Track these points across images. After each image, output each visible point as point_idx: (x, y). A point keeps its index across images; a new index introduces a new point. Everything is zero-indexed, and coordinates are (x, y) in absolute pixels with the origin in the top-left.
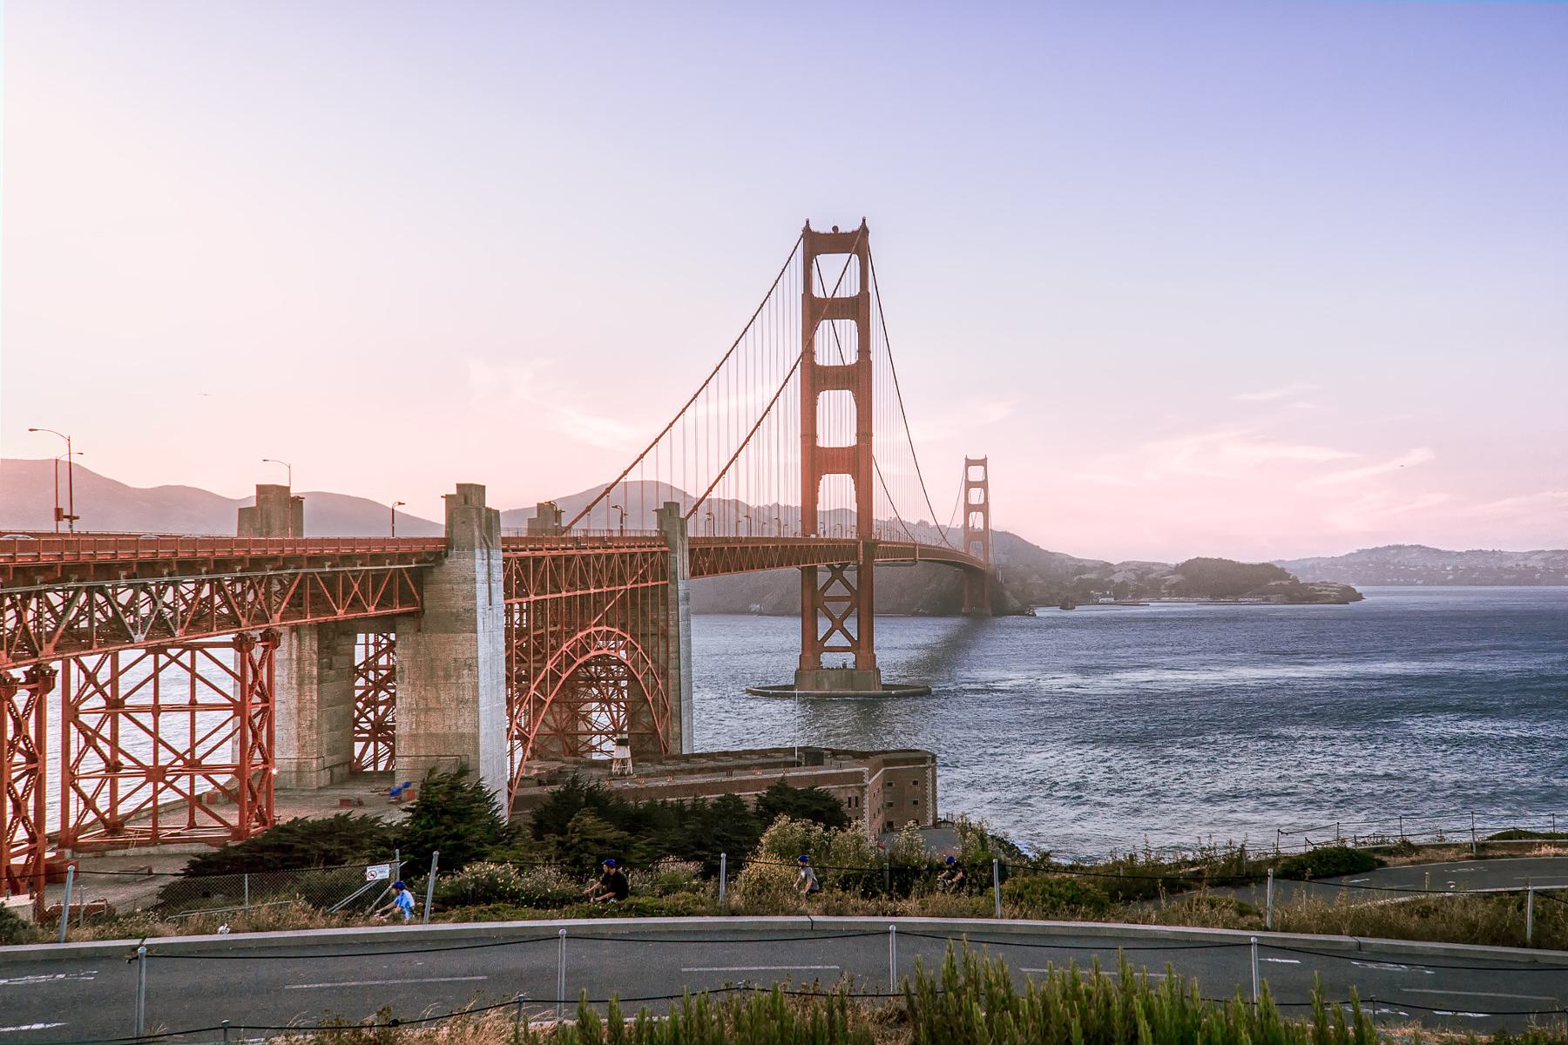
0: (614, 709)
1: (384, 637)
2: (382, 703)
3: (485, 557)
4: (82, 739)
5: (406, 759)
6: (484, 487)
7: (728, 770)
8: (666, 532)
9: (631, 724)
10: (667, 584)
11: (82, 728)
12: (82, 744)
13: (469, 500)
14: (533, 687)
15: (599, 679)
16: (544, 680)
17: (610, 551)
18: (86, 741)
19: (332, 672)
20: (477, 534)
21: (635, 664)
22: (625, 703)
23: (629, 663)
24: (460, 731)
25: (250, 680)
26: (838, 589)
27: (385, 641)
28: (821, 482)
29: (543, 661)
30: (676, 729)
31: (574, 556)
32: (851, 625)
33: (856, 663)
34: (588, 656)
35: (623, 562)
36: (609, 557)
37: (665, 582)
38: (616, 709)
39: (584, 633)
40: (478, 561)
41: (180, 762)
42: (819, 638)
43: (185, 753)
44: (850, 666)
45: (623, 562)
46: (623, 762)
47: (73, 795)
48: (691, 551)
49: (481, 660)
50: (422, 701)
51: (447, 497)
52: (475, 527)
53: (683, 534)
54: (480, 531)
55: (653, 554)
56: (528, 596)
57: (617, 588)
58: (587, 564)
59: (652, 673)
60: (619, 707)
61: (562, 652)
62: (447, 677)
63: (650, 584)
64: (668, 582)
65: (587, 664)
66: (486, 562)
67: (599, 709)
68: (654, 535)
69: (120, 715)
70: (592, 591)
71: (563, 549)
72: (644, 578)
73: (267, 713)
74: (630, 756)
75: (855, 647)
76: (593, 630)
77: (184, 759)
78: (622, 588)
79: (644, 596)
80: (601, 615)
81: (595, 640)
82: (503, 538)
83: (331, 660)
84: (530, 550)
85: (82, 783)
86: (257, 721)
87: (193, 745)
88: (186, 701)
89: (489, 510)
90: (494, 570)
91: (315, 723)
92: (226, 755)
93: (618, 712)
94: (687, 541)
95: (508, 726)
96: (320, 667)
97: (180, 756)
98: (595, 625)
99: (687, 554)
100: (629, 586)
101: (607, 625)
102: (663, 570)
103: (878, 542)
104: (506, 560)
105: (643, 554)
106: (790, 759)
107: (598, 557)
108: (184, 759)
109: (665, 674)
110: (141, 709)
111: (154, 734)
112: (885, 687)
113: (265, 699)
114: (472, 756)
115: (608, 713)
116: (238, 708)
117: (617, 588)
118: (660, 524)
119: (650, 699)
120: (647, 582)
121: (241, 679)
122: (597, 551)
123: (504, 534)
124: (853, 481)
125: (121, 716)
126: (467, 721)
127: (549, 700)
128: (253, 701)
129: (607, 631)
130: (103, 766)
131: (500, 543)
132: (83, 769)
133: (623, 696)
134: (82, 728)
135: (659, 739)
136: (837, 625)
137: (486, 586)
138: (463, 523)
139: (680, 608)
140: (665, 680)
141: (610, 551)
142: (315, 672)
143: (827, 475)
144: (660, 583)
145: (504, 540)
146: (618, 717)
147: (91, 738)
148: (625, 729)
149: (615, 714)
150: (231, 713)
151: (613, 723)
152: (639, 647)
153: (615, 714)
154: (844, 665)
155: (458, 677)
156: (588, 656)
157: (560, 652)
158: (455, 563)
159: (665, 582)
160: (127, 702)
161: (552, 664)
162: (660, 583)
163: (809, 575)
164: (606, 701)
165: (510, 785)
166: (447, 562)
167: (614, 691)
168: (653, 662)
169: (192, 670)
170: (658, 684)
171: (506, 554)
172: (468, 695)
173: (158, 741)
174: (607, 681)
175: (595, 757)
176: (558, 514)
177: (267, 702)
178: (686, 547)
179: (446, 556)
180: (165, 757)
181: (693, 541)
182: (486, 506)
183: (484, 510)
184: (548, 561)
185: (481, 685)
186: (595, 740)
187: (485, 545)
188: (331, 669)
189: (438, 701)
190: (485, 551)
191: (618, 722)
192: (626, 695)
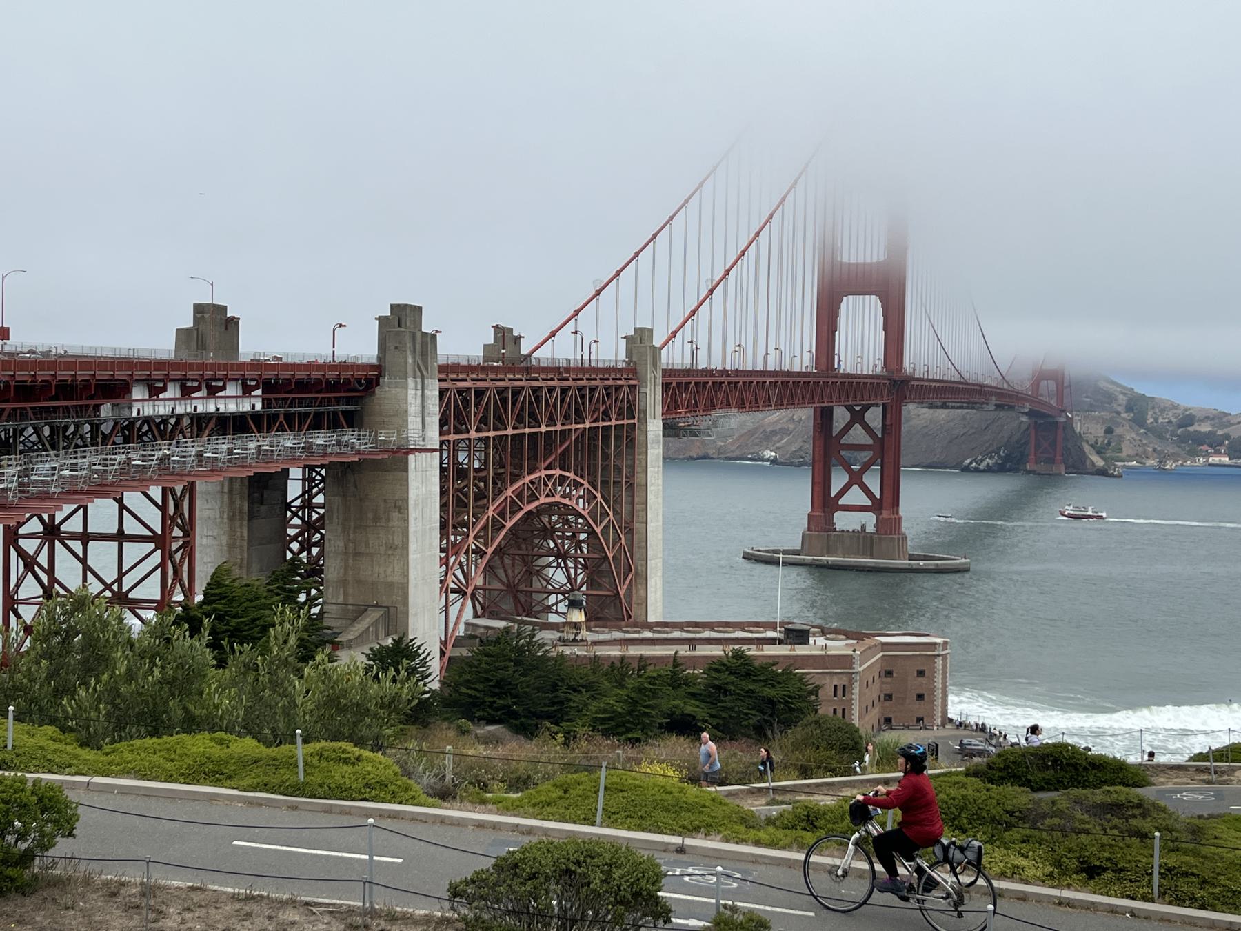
0: (570, 565)
1: (318, 473)
2: (316, 544)
3: (419, 387)
4: (21, 563)
5: (334, 607)
6: (420, 308)
7: (692, 642)
8: (635, 363)
9: (591, 582)
10: (634, 424)
11: (22, 553)
12: (21, 568)
13: (403, 324)
14: (471, 535)
15: (554, 530)
16: (485, 528)
17: (566, 383)
18: (25, 566)
19: (263, 508)
20: (410, 361)
21: (592, 513)
22: (584, 559)
23: (585, 513)
24: (389, 579)
25: (171, 511)
26: (857, 435)
27: (318, 477)
28: (843, 305)
29: (486, 508)
30: (642, 593)
31: (523, 388)
32: (873, 481)
33: (876, 526)
34: (536, 504)
35: (583, 397)
36: (564, 391)
37: (632, 421)
38: (573, 566)
39: (532, 477)
40: (411, 392)
41: (108, 594)
42: (833, 495)
43: (113, 583)
44: (870, 528)
45: (583, 397)
46: (576, 626)
47: (13, 618)
48: (666, 387)
49: (411, 502)
50: (351, 545)
51: (382, 320)
52: (408, 352)
53: (655, 365)
54: (414, 358)
55: (618, 388)
56: (468, 432)
57: (574, 426)
58: (538, 399)
59: (614, 527)
60: (576, 562)
61: (506, 498)
62: (376, 519)
63: (613, 422)
64: (635, 421)
65: (540, 511)
66: (419, 393)
67: (555, 564)
68: (624, 365)
69: (56, 541)
70: (544, 429)
71: (510, 380)
72: (606, 415)
73: (188, 547)
74: (583, 619)
75: (877, 506)
76: (543, 473)
77: (112, 591)
78: (579, 426)
79: (606, 439)
80: (554, 456)
81: (546, 485)
82: (440, 366)
83: (262, 496)
84: (473, 380)
85: (21, 609)
86: (178, 556)
87: (121, 574)
88: (114, 530)
89: (426, 334)
90: (429, 402)
91: (245, 562)
92: (151, 589)
93: (576, 569)
94: (659, 374)
95: (443, 578)
96: (251, 502)
97: (108, 587)
98: (546, 469)
99: (659, 389)
100: (588, 425)
101: (562, 469)
102: (631, 408)
103: (911, 378)
104: (442, 393)
105: (607, 388)
106: (770, 634)
107: (551, 390)
108: (112, 591)
109: (630, 531)
110: (73, 536)
111: (83, 560)
112: (911, 557)
113: (186, 534)
114: (400, 608)
115: (564, 569)
116: (160, 541)
117: (574, 426)
118: (629, 353)
119: (610, 556)
120: (610, 420)
121: (163, 508)
122: (550, 383)
123: (442, 361)
124: (879, 304)
125: (57, 542)
126: (396, 570)
127: (490, 551)
128: (173, 535)
129: (560, 475)
130: (40, 591)
131: (437, 372)
132: (22, 594)
133: (582, 551)
134: (22, 553)
135: (621, 603)
136: (856, 479)
137: (419, 419)
138: (396, 348)
139: (649, 452)
140: (629, 536)
141: (566, 383)
142: (246, 508)
143: (851, 297)
144: (626, 422)
145: (443, 369)
146: (576, 575)
147: (30, 563)
148: (584, 588)
149: (572, 571)
150: (152, 546)
151: (569, 578)
152: (599, 496)
153: (572, 571)
154: (863, 528)
155: (388, 520)
156: (536, 504)
157: (503, 498)
158: (386, 392)
159: (632, 421)
160: (63, 528)
161: (494, 511)
162: (626, 422)
163: (824, 417)
164: (561, 555)
165: (444, 643)
166: (377, 390)
167: (571, 544)
168: (616, 513)
169: (120, 501)
170: (620, 539)
171: (444, 385)
172: (398, 541)
173: (86, 568)
174: (563, 533)
175: (553, 618)
176: (517, 340)
177: (189, 536)
178: (660, 381)
179: (378, 384)
180: (95, 587)
181: (667, 373)
182: (423, 330)
183: (419, 335)
184: (491, 395)
185: (412, 528)
186: (552, 599)
187: (418, 373)
188: (262, 504)
189: (367, 546)
190: (419, 380)
191: (576, 580)
192: (585, 551)
